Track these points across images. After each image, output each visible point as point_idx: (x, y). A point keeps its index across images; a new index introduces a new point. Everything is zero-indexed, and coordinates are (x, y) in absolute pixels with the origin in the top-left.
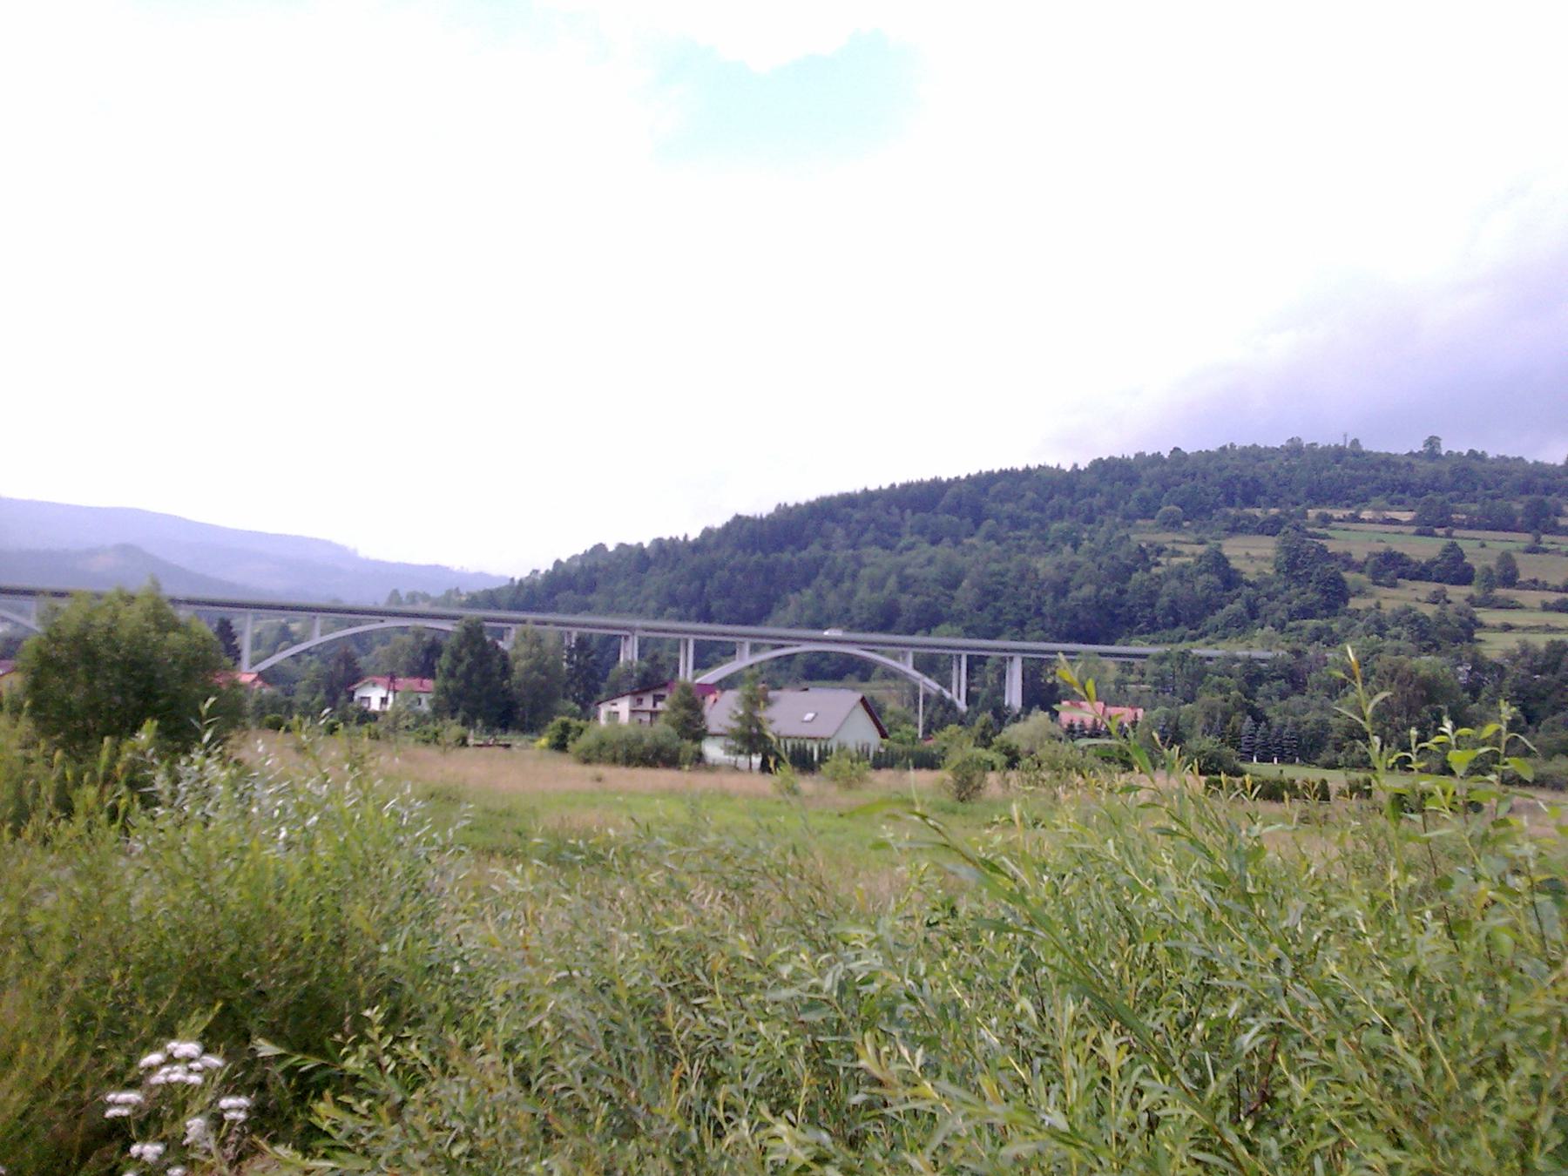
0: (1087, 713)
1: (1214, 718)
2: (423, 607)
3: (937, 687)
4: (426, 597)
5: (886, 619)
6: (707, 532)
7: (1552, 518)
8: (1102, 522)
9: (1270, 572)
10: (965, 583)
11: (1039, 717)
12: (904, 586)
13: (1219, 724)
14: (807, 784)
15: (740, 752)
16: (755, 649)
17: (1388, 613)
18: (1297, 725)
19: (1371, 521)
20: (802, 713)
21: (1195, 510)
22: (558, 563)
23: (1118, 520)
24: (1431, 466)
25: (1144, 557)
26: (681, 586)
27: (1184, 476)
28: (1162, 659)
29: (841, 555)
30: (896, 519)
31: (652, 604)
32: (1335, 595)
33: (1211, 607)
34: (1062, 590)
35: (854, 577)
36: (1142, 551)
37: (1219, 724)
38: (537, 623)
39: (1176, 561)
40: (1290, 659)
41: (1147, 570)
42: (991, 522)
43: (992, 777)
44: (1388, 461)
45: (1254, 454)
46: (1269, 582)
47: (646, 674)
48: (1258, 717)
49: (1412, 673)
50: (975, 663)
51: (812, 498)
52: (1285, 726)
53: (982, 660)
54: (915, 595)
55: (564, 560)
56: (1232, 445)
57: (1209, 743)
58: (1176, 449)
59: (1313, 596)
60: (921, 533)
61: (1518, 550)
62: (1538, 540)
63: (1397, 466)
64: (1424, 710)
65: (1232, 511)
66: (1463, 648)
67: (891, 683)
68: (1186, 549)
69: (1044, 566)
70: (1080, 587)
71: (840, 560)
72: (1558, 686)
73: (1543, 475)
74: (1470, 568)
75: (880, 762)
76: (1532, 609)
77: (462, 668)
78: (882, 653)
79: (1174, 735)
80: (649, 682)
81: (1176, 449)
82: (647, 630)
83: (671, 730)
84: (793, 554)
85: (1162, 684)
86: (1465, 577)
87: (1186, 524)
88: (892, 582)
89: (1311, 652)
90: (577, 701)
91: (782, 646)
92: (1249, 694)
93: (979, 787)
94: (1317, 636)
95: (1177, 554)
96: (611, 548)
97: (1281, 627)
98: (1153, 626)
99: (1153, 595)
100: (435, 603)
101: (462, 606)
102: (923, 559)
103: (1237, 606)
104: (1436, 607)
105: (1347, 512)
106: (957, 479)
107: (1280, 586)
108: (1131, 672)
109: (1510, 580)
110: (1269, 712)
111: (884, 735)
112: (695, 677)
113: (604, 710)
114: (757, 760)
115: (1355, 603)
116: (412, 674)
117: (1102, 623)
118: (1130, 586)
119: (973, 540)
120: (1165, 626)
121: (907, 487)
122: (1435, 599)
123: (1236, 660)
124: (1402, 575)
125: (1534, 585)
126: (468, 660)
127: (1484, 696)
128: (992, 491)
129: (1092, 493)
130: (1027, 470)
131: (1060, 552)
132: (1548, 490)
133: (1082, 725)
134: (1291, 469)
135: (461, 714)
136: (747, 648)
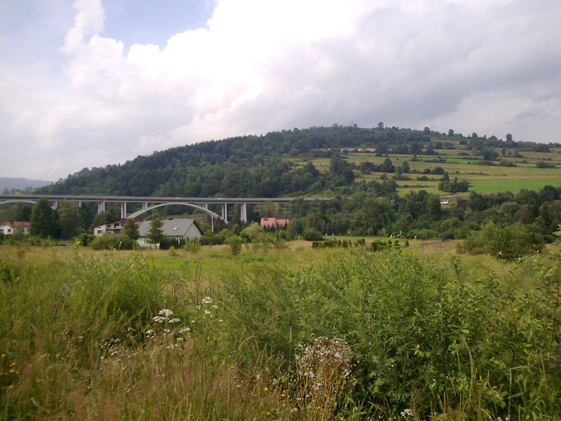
0: (271, 222)
1: (312, 221)
2: (18, 194)
3: (217, 216)
4: (18, 191)
5: (197, 192)
6: (128, 162)
7: (420, 149)
8: (271, 155)
9: (329, 170)
10: (225, 178)
11: (254, 225)
12: (202, 180)
13: (314, 223)
14: (180, 252)
15: (152, 243)
16: (149, 205)
17: (367, 183)
18: (339, 222)
19: (361, 152)
20: (173, 227)
21: (303, 150)
22: (70, 176)
23: (277, 154)
24: (380, 132)
25: (286, 167)
26: (120, 183)
27: (299, 138)
28: (294, 202)
29: (179, 170)
30: (199, 156)
31: (109, 190)
32: (350, 177)
33: (310, 183)
34: (258, 179)
35: (184, 177)
36: (286, 165)
37: (314, 223)
38: (68, 199)
39: (297, 168)
40: (336, 200)
41: (287, 171)
42: (233, 156)
43: (243, 246)
44: (366, 131)
45: (322, 130)
46: (328, 174)
47: (110, 216)
48: (327, 220)
49: (376, 204)
50: (230, 206)
51: (167, 149)
52: (335, 223)
53: (232, 205)
54: (207, 183)
55: (72, 174)
56: (315, 127)
57: (312, 230)
58: (296, 128)
59: (343, 178)
60: (208, 160)
61: (409, 160)
62: (416, 157)
63: (370, 133)
64: (380, 215)
65: (315, 150)
66: (392, 194)
67: (200, 215)
68: (300, 163)
69: (252, 171)
70: (265, 178)
71: (179, 171)
72: (423, 205)
73: (417, 135)
74: (393, 167)
75: (204, 242)
76: (414, 180)
77: (40, 217)
78: (196, 204)
79: (299, 230)
80: (112, 218)
81: (296, 128)
82: (108, 200)
83: (127, 236)
84: (161, 169)
85: (294, 210)
86: (392, 170)
87: (300, 155)
88: (198, 179)
89: (343, 197)
90: (83, 227)
91: (159, 204)
92: (324, 213)
93: (239, 249)
94: (345, 192)
95: (298, 165)
96: (90, 169)
97: (333, 189)
98: (290, 191)
99: (290, 180)
100: (22, 192)
101: (34, 193)
102: (208, 169)
103: (318, 183)
104: (383, 181)
105: (353, 149)
106: (220, 140)
107: (332, 175)
108: (284, 207)
109: (407, 170)
110: (330, 219)
111: (202, 234)
112: (127, 216)
113: (96, 230)
114: (158, 245)
115: (357, 180)
116: (19, 220)
117: (274, 190)
118: (282, 177)
119: (227, 163)
120: (295, 190)
121: (202, 144)
122: (383, 178)
123: (318, 201)
124: (372, 170)
125: (415, 172)
126: (42, 214)
127: (399, 210)
128: (233, 145)
129: (268, 144)
130: (245, 137)
131: (257, 166)
132: (418, 140)
133: (269, 226)
134: (335, 135)
135: (41, 234)
136: (146, 204)
